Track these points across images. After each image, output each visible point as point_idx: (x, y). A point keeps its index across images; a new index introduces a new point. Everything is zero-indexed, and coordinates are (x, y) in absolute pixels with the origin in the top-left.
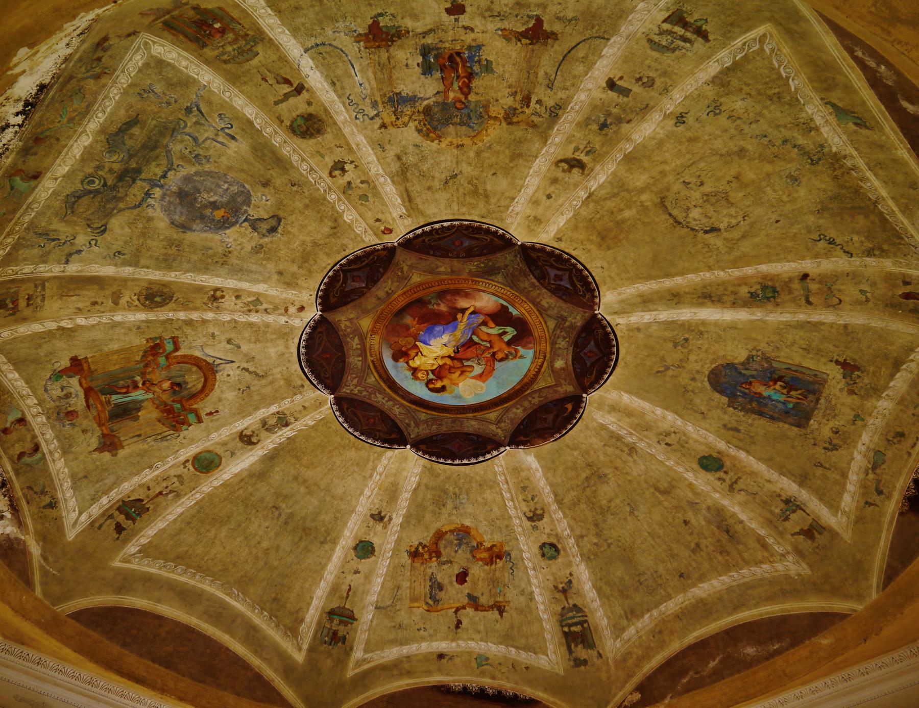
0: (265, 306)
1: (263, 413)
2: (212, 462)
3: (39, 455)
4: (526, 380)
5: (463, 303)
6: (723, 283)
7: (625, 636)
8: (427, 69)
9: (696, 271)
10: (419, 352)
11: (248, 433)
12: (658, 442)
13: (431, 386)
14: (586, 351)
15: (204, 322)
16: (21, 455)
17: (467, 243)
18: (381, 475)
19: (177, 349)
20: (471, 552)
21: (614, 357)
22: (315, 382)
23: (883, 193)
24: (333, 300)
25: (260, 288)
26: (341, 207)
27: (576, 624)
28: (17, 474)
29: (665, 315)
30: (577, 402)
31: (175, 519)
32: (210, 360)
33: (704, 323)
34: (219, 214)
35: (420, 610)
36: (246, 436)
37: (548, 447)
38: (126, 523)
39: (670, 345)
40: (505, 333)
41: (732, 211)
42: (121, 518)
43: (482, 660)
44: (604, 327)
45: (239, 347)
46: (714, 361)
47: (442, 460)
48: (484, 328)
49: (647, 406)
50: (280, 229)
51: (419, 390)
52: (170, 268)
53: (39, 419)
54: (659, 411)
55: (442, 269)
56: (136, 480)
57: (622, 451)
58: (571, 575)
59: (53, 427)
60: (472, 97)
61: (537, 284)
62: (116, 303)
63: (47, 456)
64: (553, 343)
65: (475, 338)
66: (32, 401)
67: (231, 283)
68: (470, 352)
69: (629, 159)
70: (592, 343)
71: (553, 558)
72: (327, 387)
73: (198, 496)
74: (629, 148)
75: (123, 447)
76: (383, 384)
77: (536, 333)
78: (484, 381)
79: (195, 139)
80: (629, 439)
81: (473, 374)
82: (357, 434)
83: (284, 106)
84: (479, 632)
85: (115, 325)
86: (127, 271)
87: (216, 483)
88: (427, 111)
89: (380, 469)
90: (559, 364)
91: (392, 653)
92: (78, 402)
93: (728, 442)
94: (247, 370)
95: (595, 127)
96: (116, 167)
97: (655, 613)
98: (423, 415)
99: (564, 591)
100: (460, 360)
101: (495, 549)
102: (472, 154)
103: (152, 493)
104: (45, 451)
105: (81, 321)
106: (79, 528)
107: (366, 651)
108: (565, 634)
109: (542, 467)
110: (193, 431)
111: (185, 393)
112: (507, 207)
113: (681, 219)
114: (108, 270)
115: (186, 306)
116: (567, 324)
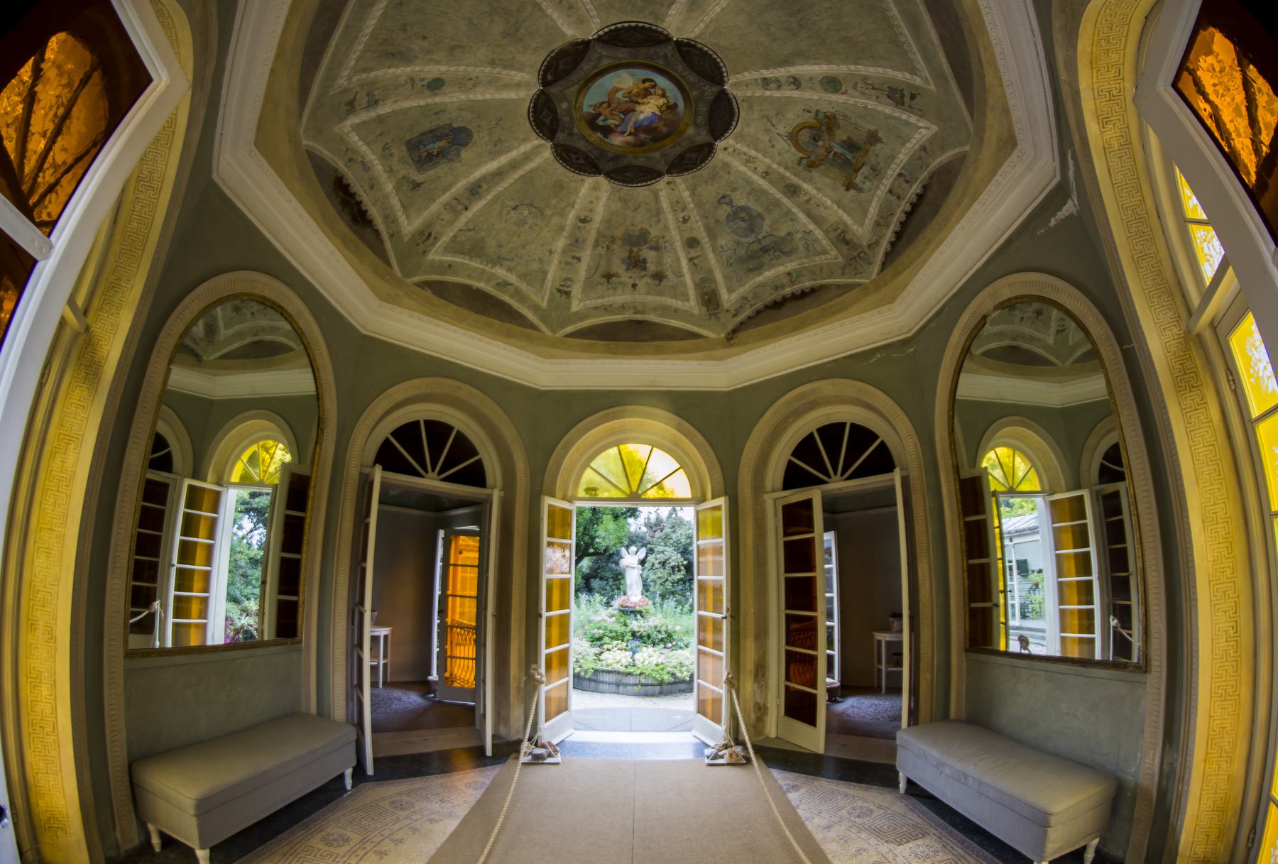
0: (745, 157)
1: (777, 94)
2: (828, 82)
3: (904, 172)
4: (585, 90)
5: (630, 139)
6: (496, 185)
8: (645, 261)
9: (511, 185)
10: (660, 108)
11: (793, 86)
12: (477, 77)
13: (653, 84)
14: (550, 118)
15: (779, 164)
16: (907, 182)
17: (629, 174)
18: (703, 20)
19: (801, 158)
21: (531, 119)
22: (734, 100)
23: (472, 264)
24: (707, 149)
25: (742, 168)
26: (689, 199)
28: (916, 180)
29: (513, 154)
30: (545, 83)
32: (789, 142)
33: (492, 159)
34: (743, 215)
36: (795, 85)
37: (558, 44)
39: (503, 139)
40: (604, 121)
41: (513, 220)
42: (907, 99)
44: (544, 135)
45: (770, 141)
46: (475, 143)
47: (647, 26)
48: (617, 123)
49: (497, 96)
50: (720, 196)
51: (662, 81)
52: (778, 200)
53: (886, 183)
54: (488, 97)
55: (643, 159)
56: (879, 108)
57: (500, 60)
59: (886, 173)
60: (628, 248)
61: (589, 153)
62: (810, 200)
63: (901, 166)
64: (572, 118)
65: (623, 116)
66: (879, 192)
67: (755, 178)
68: (624, 107)
69: (562, 228)
70: (548, 123)
72: (727, 95)
73: (852, 67)
74: (564, 233)
75: (869, 130)
76: (689, 90)
77: (583, 124)
78: (615, 87)
79: (735, 252)
80: (497, 70)
81: (622, 92)
82: (715, 56)
83: (698, 254)
85: (819, 190)
86: (794, 210)
87: (835, 67)
88: (646, 243)
89: (702, 25)
90: (565, 105)
92: (865, 170)
93: (436, 104)
94: (773, 125)
95: (580, 240)
96: (766, 256)
98: (660, 63)
100: (632, 101)
102: (628, 221)
103: (878, 93)
104: (899, 168)
105: (829, 203)
106: (928, 124)
109: (559, 28)
110: (826, 108)
111: (815, 132)
112: (610, 195)
113: (531, 208)
114: (802, 216)
115: (782, 177)
116: (566, 132)
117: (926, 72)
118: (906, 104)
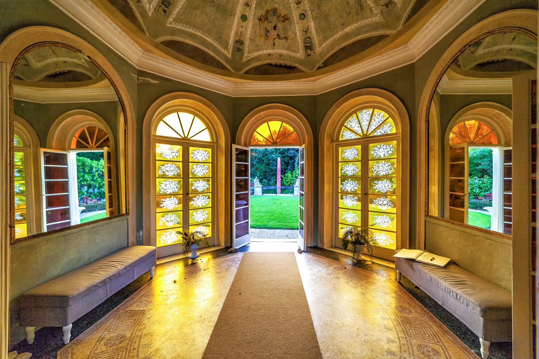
7: (322, 46)
20: (278, 18)
27: (308, 43)
31: (181, 7)
35: (263, 39)
38: (166, 9)
43: (281, 55)
58: (308, 25)
71: (303, 19)
84: (280, 46)
91: (256, 54)
97: (332, 38)
99: (306, 32)
101: (285, 17)
107: (248, 54)
108: (305, 46)
117: (174, 26)
118: (162, 5)
